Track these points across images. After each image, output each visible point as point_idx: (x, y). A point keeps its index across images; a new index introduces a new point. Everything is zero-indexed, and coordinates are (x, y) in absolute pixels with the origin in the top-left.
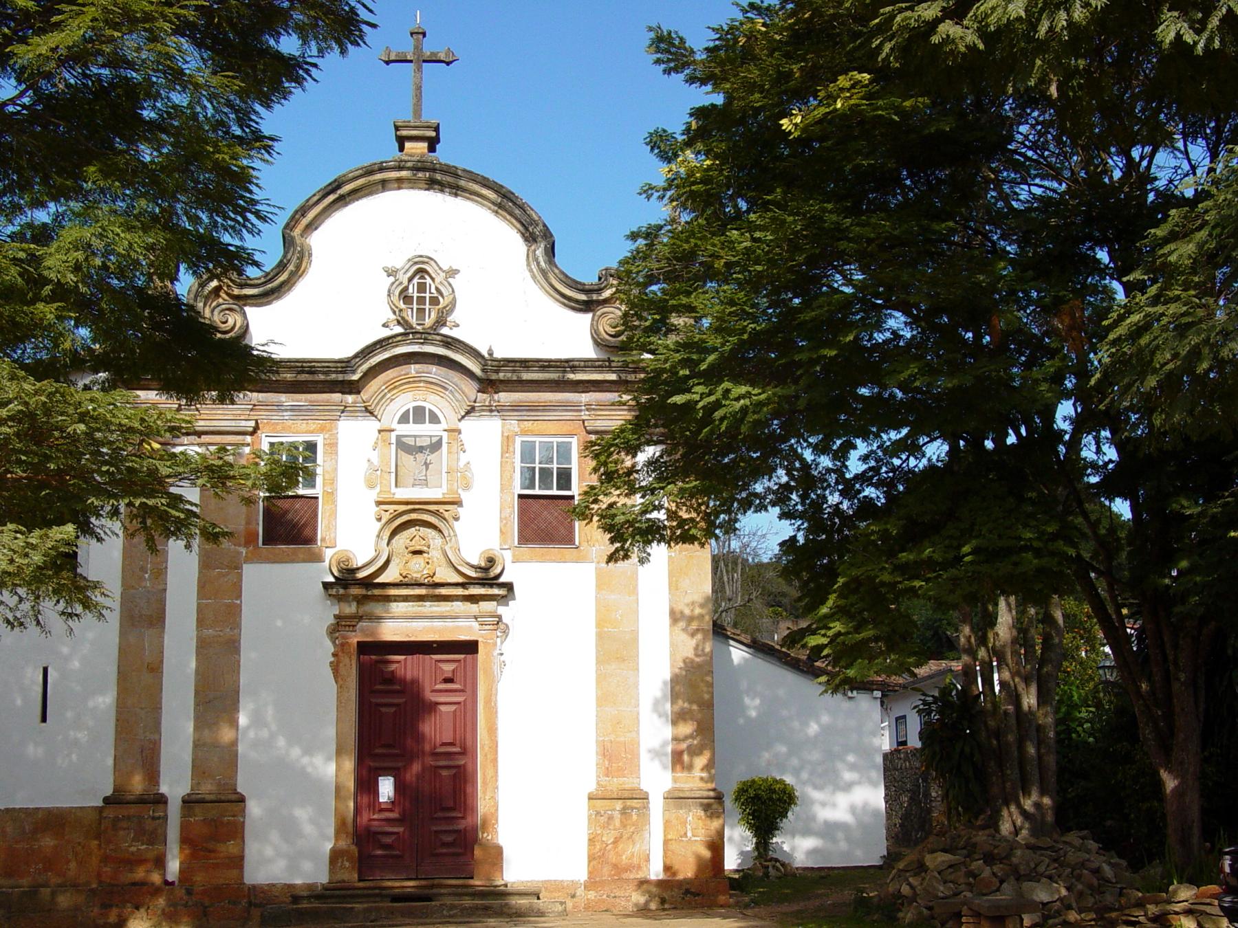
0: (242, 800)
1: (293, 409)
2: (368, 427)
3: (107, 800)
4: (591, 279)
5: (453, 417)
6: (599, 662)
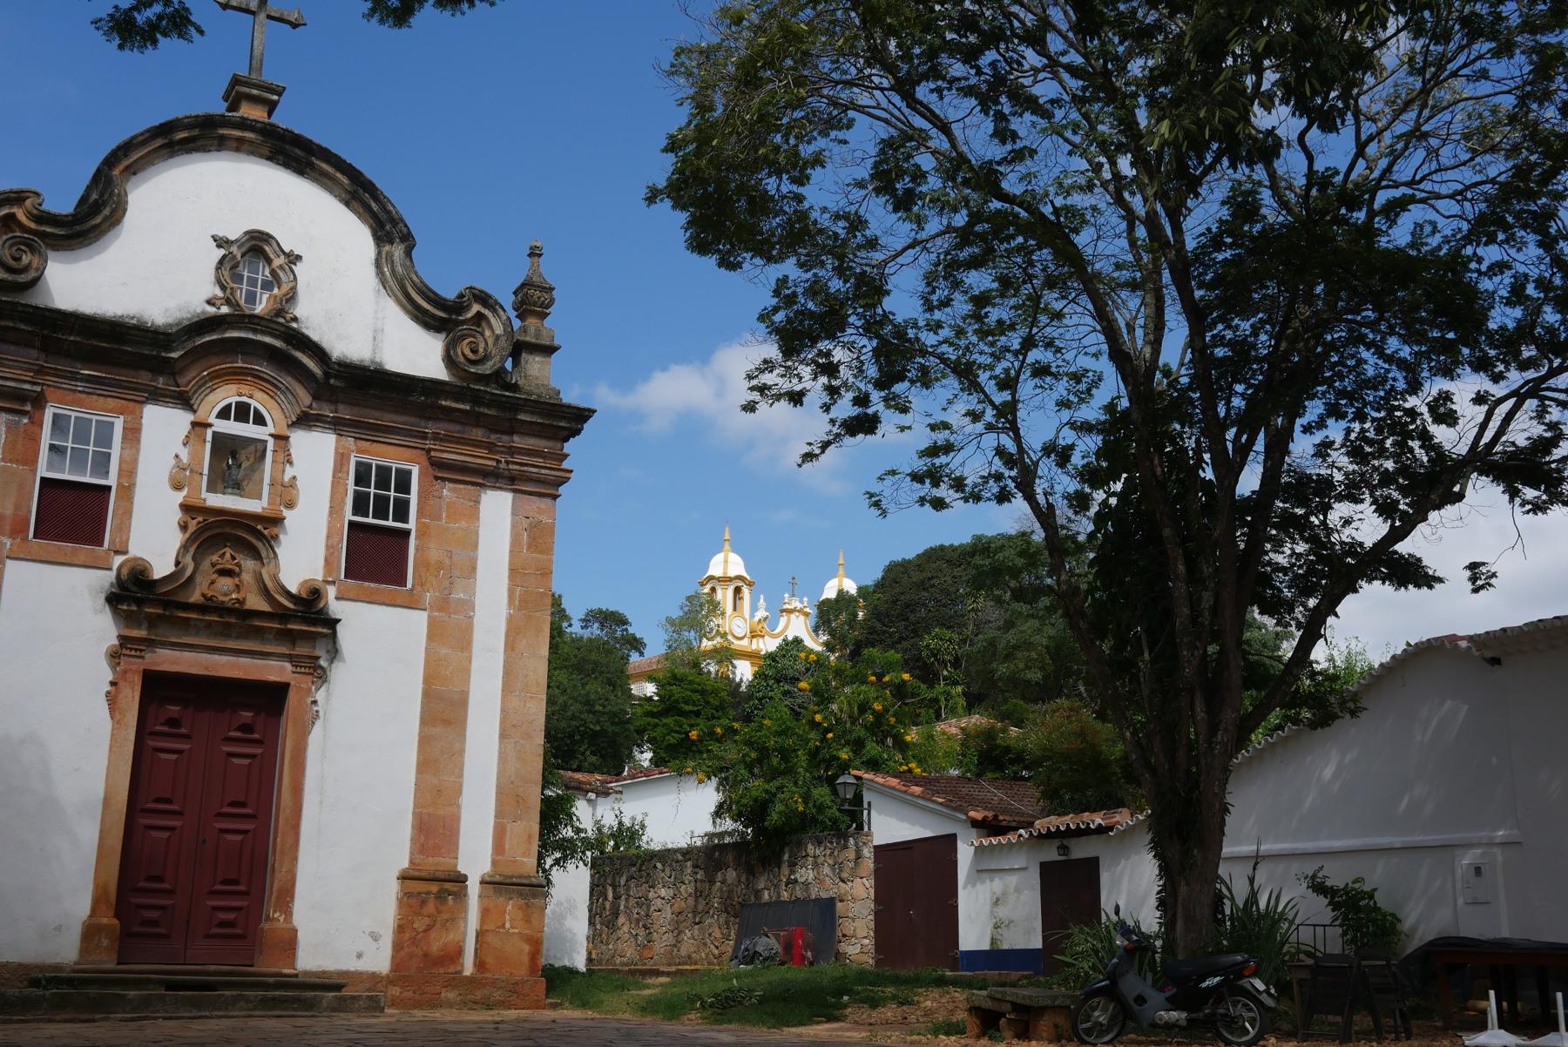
1: (89, 379)
2: (180, 420)
4: (450, 294)
5: (283, 423)
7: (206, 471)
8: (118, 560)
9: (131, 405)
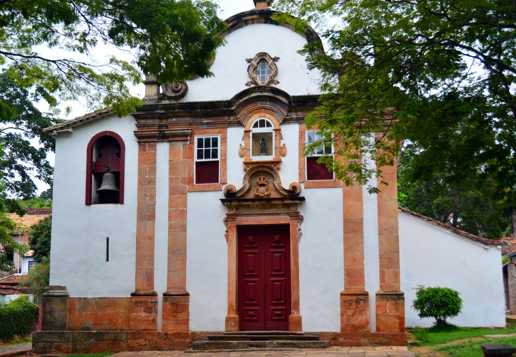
0: (188, 295)
1: (207, 124)
3: (132, 295)
5: (277, 124)
6: (345, 232)
7: (251, 148)
8: (224, 187)
9: (223, 129)
